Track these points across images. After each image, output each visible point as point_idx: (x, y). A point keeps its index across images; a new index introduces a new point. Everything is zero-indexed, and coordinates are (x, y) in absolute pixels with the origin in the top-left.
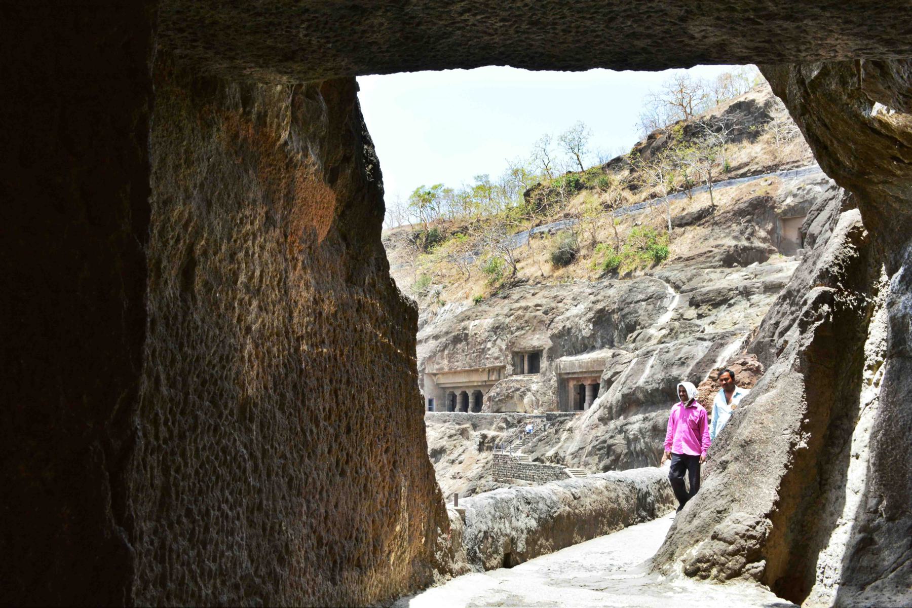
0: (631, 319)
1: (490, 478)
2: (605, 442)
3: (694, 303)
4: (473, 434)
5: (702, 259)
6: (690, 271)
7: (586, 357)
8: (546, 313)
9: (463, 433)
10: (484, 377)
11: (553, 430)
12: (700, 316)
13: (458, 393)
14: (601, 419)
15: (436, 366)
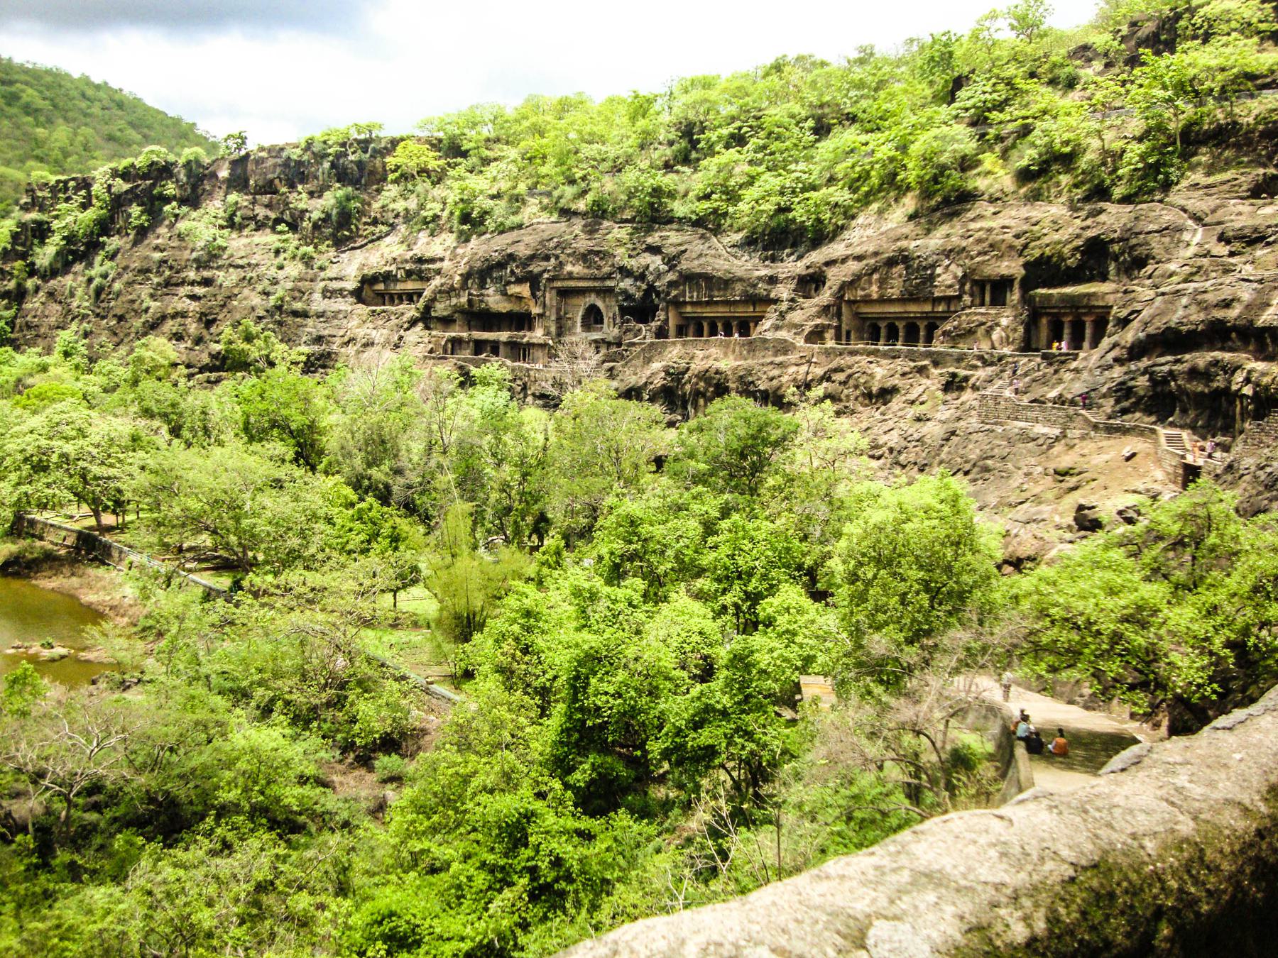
0: (1142, 251)
1: (973, 420)
2: (1123, 383)
3: (1223, 238)
4: (935, 372)
5: (1226, 187)
6: (1212, 202)
7: (1068, 290)
8: (1017, 236)
9: (921, 370)
10: (928, 308)
11: (1051, 370)
12: (1232, 254)
13: (883, 325)
14: (1115, 360)
15: (860, 293)
